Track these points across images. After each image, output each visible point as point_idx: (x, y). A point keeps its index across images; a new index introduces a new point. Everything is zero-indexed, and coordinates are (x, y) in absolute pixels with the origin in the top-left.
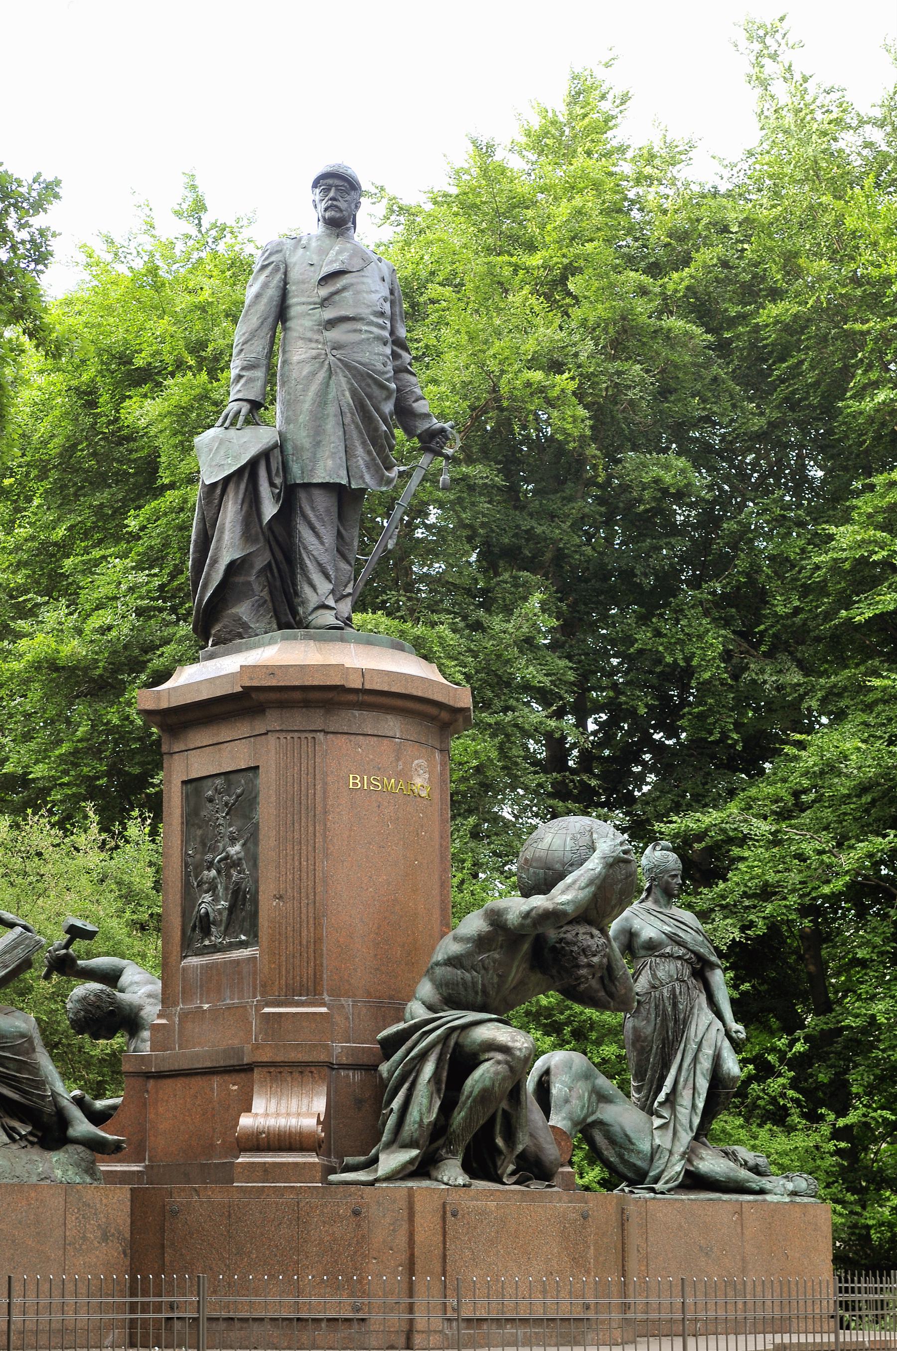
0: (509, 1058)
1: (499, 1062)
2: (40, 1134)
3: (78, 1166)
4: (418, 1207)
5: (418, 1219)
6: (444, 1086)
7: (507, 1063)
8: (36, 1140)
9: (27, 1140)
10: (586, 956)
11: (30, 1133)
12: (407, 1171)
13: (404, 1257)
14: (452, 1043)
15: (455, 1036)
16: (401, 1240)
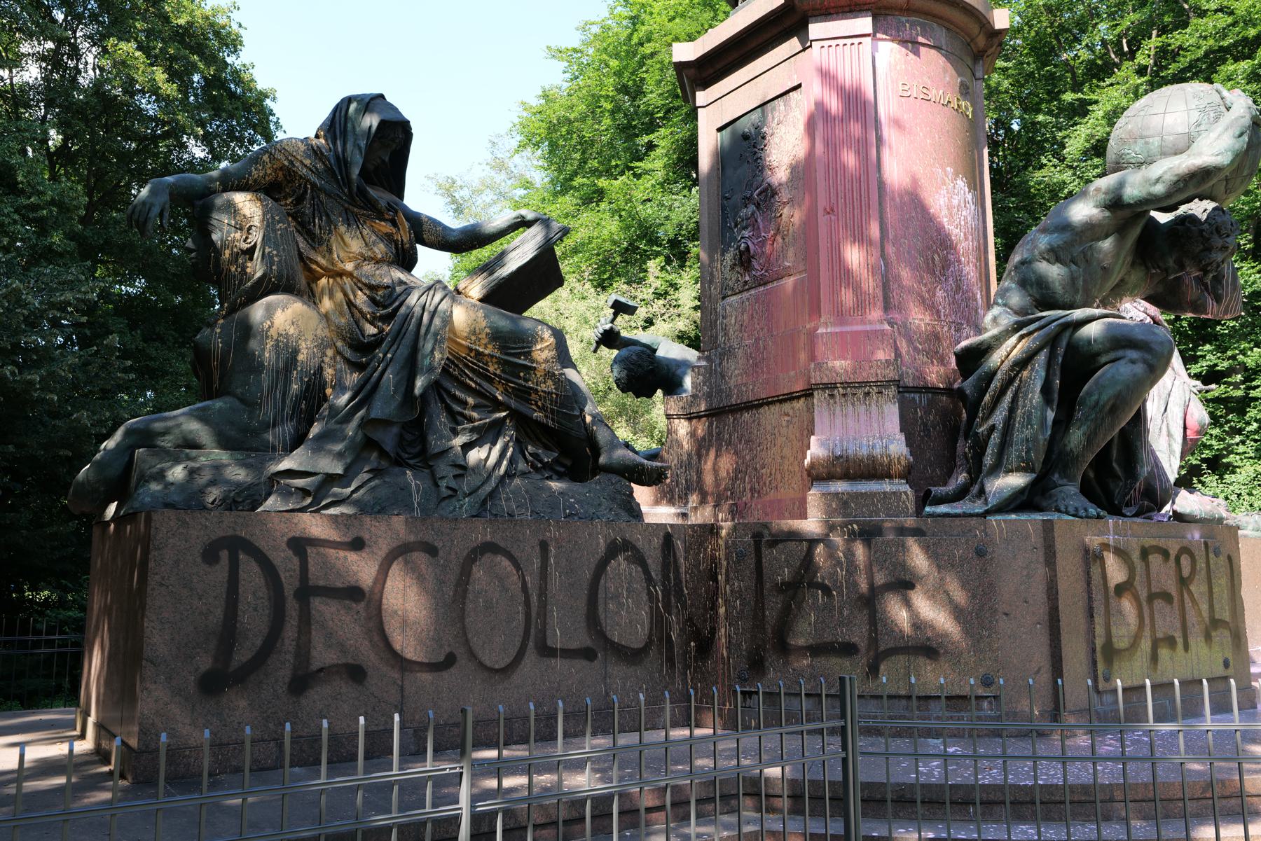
0: (1148, 357)
1: (1133, 362)
2: (568, 462)
3: (613, 500)
4: (1059, 545)
5: (1060, 562)
6: (1056, 396)
7: (1145, 361)
8: (562, 470)
9: (552, 469)
10: (1220, 235)
11: (556, 461)
12: (1018, 502)
13: (1042, 610)
14: (1064, 343)
15: (1067, 334)
16: (1038, 591)
